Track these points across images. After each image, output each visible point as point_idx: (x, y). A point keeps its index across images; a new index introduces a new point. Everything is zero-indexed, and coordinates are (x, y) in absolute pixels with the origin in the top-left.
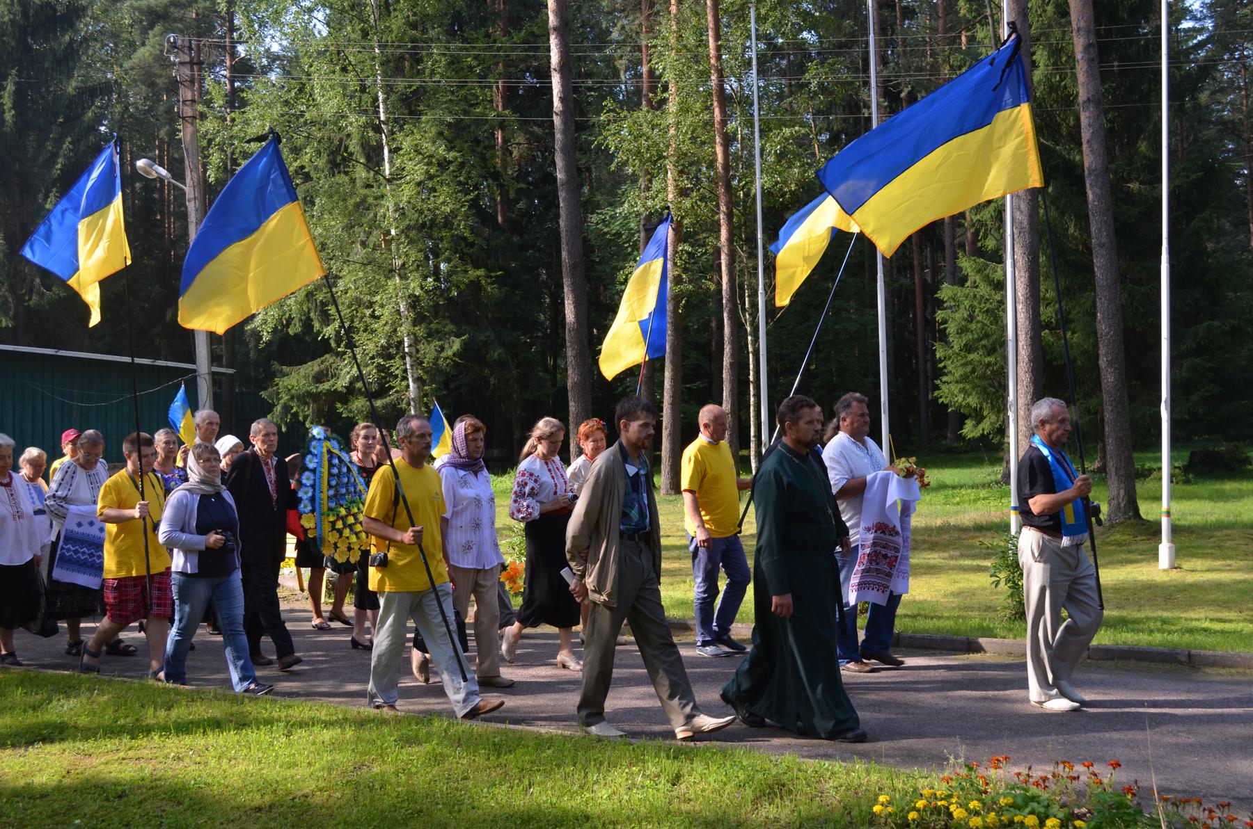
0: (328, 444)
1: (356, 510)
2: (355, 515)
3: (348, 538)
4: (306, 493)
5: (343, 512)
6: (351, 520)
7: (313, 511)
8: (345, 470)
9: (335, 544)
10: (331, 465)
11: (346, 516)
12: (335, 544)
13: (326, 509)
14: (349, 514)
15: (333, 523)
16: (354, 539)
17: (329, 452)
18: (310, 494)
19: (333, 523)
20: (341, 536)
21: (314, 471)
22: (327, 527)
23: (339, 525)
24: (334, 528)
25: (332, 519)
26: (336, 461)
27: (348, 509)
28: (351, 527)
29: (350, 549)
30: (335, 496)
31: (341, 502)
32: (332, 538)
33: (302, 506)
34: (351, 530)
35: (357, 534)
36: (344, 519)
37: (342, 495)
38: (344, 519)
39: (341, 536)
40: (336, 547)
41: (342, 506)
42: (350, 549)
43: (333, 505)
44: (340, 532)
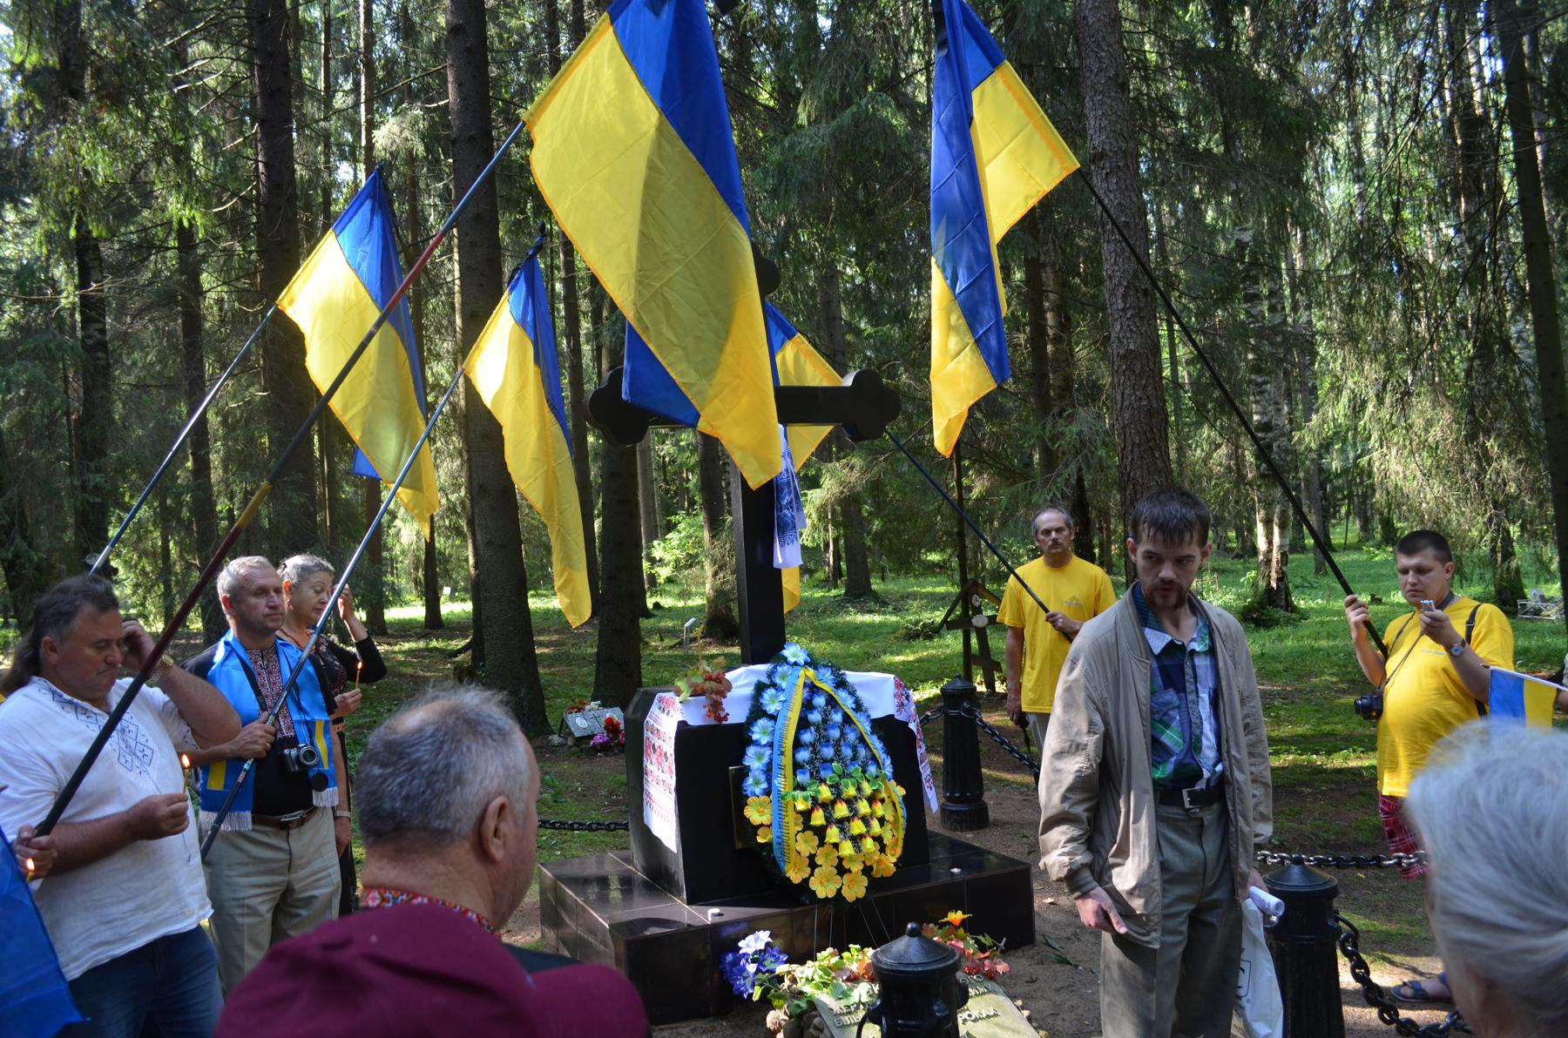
0: (811, 672)
1: (851, 791)
2: (850, 802)
3: (836, 846)
4: (759, 757)
5: (825, 793)
6: (841, 810)
7: (768, 792)
8: (838, 717)
9: (812, 857)
10: (808, 706)
11: (833, 803)
12: (812, 857)
13: (790, 783)
14: (838, 796)
15: (807, 815)
16: (847, 849)
17: (812, 689)
18: (765, 760)
19: (807, 815)
20: (822, 843)
21: (773, 717)
22: (793, 825)
23: (818, 818)
24: (807, 826)
25: (801, 806)
26: (820, 701)
27: (836, 788)
28: (842, 823)
29: (841, 870)
30: (811, 761)
31: (823, 773)
32: (805, 845)
33: (750, 781)
34: (842, 830)
35: (856, 840)
36: (827, 806)
37: (825, 761)
38: (827, 806)
39: (822, 843)
40: (813, 865)
41: (823, 781)
42: (841, 870)
43: (802, 778)
44: (820, 832)
